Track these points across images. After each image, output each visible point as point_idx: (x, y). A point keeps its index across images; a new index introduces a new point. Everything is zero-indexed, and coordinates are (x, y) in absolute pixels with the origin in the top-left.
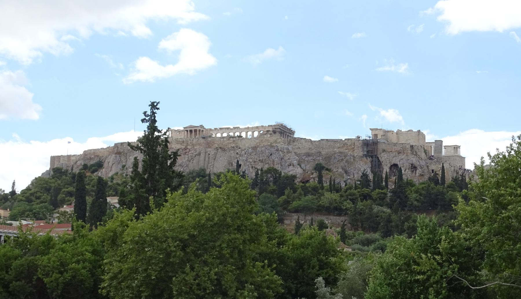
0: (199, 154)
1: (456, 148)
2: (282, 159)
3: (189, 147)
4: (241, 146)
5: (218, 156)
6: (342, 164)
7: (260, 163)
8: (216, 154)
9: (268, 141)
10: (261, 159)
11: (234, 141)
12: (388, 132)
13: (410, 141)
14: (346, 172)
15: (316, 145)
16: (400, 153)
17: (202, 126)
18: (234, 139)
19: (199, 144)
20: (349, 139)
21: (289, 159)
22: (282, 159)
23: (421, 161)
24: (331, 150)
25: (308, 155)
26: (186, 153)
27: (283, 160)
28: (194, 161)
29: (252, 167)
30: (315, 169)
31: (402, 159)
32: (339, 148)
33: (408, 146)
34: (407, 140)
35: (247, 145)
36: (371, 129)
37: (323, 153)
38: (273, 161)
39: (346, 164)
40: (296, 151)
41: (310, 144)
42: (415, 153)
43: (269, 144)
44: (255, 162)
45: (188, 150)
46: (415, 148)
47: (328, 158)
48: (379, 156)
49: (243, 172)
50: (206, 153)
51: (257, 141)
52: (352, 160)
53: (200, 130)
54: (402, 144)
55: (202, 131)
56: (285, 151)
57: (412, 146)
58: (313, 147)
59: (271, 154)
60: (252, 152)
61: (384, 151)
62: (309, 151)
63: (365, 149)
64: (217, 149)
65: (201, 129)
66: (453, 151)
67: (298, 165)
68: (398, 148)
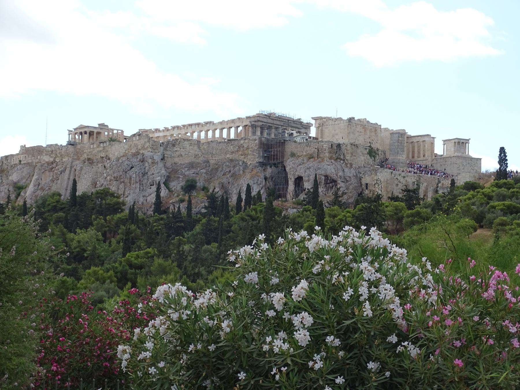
1: (461, 144)
2: (144, 174)
3: (57, 160)
11: (104, 147)
13: (337, 137)
19: (68, 155)
23: (346, 170)
26: (52, 168)
27: (146, 177)
28: (59, 182)
31: (310, 168)
32: (233, 152)
37: (212, 162)
38: (130, 179)
41: (196, 147)
45: (54, 165)
46: (343, 148)
50: (71, 167)
57: (339, 145)
61: (293, 155)
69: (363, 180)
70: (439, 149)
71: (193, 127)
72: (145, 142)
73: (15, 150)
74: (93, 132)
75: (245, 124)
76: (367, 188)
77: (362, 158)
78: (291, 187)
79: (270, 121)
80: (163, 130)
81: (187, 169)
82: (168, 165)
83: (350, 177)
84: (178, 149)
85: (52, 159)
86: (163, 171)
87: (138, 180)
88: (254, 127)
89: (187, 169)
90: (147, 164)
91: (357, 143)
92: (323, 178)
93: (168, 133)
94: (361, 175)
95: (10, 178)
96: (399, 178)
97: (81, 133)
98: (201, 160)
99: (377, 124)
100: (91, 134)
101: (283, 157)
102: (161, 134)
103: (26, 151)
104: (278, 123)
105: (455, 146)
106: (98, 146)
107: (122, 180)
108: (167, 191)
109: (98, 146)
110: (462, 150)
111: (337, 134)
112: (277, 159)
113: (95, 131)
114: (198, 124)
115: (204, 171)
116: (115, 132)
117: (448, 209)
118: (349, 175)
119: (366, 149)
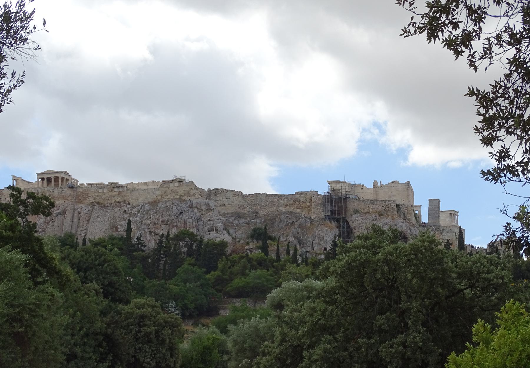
0: (64, 213)
4: (131, 201)
5: (94, 215)
6: (293, 230)
7: (163, 226)
8: (90, 213)
9: (175, 192)
10: (165, 219)
11: (120, 193)
12: (356, 186)
14: (300, 242)
15: (250, 200)
16: (382, 215)
17: (65, 173)
18: (121, 189)
19: (64, 198)
20: (301, 193)
21: (209, 220)
22: (199, 220)
23: (412, 229)
24: (275, 208)
25: (238, 216)
27: (200, 222)
28: (55, 224)
29: (151, 232)
30: (252, 237)
32: (286, 206)
33: (393, 205)
34: (390, 197)
35: (141, 199)
36: (329, 183)
37: (262, 213)
39: (300, 230)
40: (219, 209)
41: (240, 198)
42: (402, 216)
43: (178, 197)
44: (155, 224)
46: (403, 209)
47: (271, 220)
48: (349, 220)
49: (137, 239)
50: (74, 210)
51: (158, 193)
52: (309, 224)
53: (63, 178)
54: (385, 201)
55: (67, 180)
56: (204, 207)
58: (245, 205)
59: (181, 213)
60: (150, 209)
61: (356, 211)
62: (238, 210)
63: (329, 208)
64: (92, 205)
65: (66, 177)
66: (448, 219)
67: (226, 229)
68: (379, 207)
84: (221, 199)
87: (194, 225)
89: (233, 218)
107: (175, 224)
112: (338, 214)
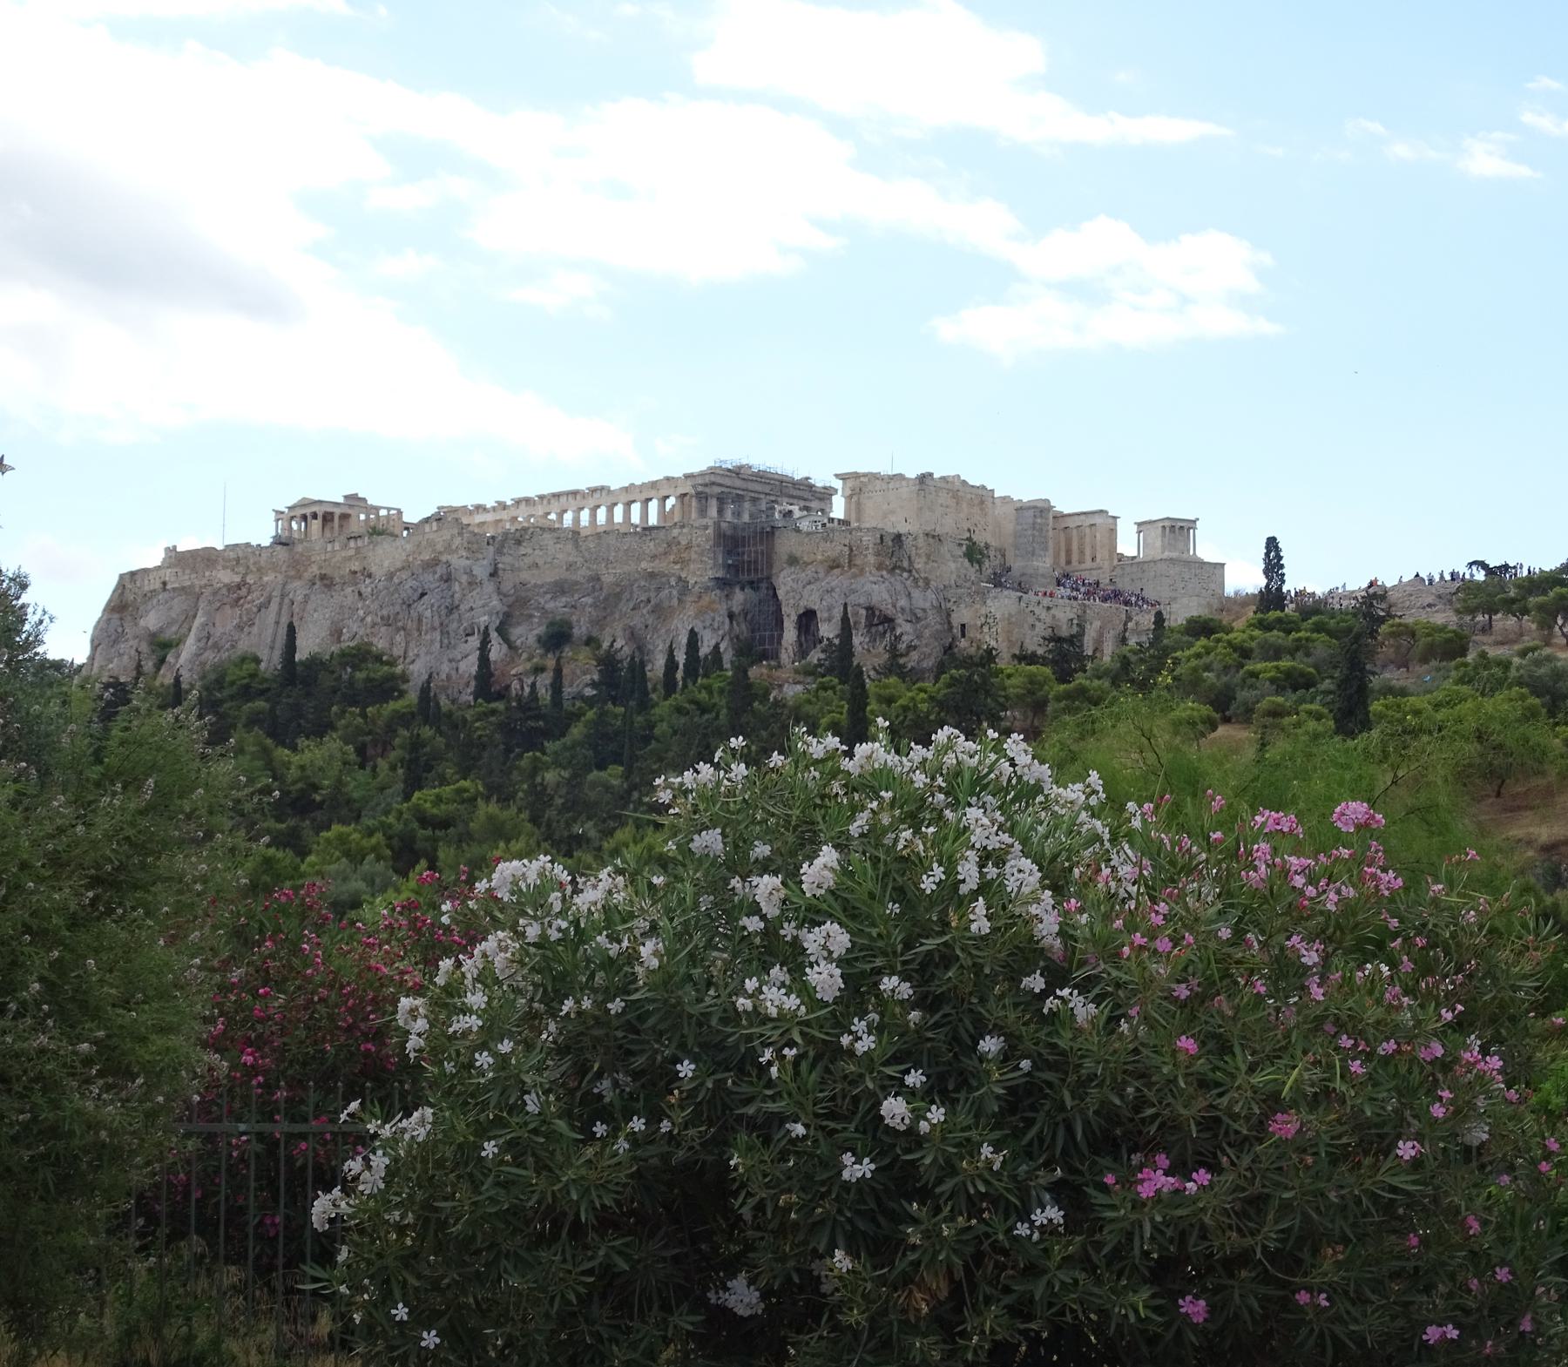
1: (1178, 530)
2: (452, 609)
3: (250, 579)
7: (383, 629)
11: (358, 549)
19: (275, 567)
23: (916, 593)
26: (239, 598)
27: (455, 616)
28: (255, 630)
32: (654, 557)
37: (608, 579)
38: (420, 620)
41: (569, 547)
45: (244, 591)
46: (908, 542)
50: (283, 596)
57: (898, 538)
61: (793, 561)
69: (954, 615)
70: (1128, 544)
71: (563, 499)
72: (453, 537)
73: (153, 558)
74: (332, 514)
75: (681, 491)
76: (963, 635)
77: (953, 566)
78: (790, 634)
79: (738, 483)
80: (494, 509)
81: (549, 596)
82: (507, 586)
83: (924, 610)
84: (529, 551)
85: (237, 579)
86: (495, 602)
87: (437, 624)
88: (702, 497)
89: (549, 596)
90: (457, 587)
91: (939, 531)
92: (864, 612)
93: (504, 515)
94: (949, 605)
95: (142, 623)
96: (1037, 611)
97: (304, 518)
98: (581, 574)
99: (984, 487)
100: (327, 518)
101: (770, 566)
102: (489, 517)
103: (176, 559)
104: (758, 487)
105: (1164, 535)
106: (345, 547)
108: (505, 646)
109: (345, 547)
110: (1181, 545)
111: (893, 512)
112: (756, 570)
113: (337, 511)
114: (574, 493)
115: (589, 600)
116: (383, 513)
117: (1146, 680)
118: (921, 604)
119: (960, 545)
